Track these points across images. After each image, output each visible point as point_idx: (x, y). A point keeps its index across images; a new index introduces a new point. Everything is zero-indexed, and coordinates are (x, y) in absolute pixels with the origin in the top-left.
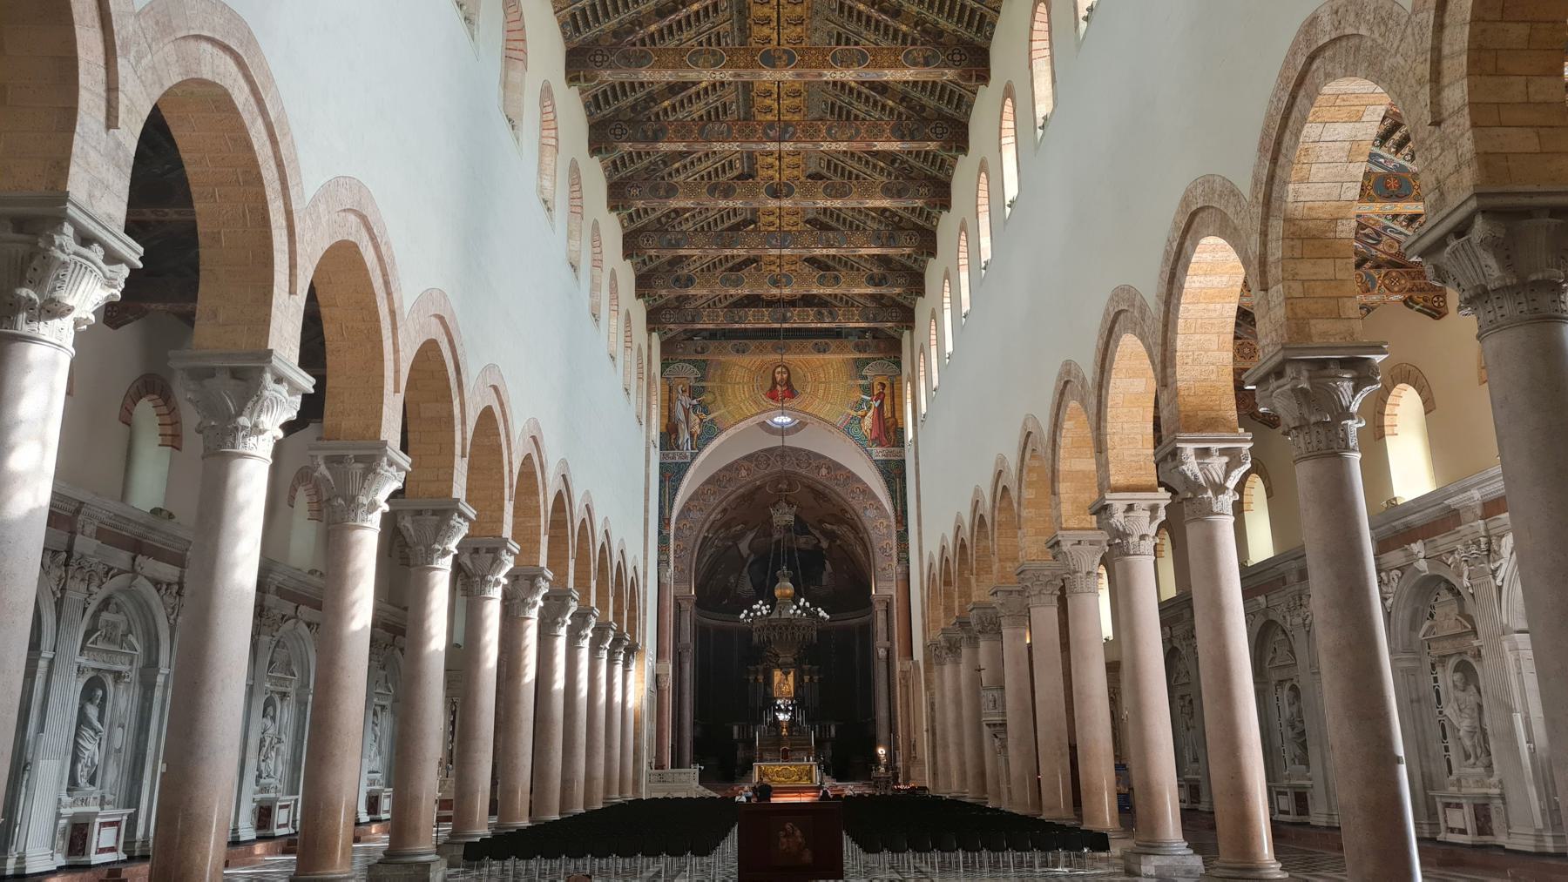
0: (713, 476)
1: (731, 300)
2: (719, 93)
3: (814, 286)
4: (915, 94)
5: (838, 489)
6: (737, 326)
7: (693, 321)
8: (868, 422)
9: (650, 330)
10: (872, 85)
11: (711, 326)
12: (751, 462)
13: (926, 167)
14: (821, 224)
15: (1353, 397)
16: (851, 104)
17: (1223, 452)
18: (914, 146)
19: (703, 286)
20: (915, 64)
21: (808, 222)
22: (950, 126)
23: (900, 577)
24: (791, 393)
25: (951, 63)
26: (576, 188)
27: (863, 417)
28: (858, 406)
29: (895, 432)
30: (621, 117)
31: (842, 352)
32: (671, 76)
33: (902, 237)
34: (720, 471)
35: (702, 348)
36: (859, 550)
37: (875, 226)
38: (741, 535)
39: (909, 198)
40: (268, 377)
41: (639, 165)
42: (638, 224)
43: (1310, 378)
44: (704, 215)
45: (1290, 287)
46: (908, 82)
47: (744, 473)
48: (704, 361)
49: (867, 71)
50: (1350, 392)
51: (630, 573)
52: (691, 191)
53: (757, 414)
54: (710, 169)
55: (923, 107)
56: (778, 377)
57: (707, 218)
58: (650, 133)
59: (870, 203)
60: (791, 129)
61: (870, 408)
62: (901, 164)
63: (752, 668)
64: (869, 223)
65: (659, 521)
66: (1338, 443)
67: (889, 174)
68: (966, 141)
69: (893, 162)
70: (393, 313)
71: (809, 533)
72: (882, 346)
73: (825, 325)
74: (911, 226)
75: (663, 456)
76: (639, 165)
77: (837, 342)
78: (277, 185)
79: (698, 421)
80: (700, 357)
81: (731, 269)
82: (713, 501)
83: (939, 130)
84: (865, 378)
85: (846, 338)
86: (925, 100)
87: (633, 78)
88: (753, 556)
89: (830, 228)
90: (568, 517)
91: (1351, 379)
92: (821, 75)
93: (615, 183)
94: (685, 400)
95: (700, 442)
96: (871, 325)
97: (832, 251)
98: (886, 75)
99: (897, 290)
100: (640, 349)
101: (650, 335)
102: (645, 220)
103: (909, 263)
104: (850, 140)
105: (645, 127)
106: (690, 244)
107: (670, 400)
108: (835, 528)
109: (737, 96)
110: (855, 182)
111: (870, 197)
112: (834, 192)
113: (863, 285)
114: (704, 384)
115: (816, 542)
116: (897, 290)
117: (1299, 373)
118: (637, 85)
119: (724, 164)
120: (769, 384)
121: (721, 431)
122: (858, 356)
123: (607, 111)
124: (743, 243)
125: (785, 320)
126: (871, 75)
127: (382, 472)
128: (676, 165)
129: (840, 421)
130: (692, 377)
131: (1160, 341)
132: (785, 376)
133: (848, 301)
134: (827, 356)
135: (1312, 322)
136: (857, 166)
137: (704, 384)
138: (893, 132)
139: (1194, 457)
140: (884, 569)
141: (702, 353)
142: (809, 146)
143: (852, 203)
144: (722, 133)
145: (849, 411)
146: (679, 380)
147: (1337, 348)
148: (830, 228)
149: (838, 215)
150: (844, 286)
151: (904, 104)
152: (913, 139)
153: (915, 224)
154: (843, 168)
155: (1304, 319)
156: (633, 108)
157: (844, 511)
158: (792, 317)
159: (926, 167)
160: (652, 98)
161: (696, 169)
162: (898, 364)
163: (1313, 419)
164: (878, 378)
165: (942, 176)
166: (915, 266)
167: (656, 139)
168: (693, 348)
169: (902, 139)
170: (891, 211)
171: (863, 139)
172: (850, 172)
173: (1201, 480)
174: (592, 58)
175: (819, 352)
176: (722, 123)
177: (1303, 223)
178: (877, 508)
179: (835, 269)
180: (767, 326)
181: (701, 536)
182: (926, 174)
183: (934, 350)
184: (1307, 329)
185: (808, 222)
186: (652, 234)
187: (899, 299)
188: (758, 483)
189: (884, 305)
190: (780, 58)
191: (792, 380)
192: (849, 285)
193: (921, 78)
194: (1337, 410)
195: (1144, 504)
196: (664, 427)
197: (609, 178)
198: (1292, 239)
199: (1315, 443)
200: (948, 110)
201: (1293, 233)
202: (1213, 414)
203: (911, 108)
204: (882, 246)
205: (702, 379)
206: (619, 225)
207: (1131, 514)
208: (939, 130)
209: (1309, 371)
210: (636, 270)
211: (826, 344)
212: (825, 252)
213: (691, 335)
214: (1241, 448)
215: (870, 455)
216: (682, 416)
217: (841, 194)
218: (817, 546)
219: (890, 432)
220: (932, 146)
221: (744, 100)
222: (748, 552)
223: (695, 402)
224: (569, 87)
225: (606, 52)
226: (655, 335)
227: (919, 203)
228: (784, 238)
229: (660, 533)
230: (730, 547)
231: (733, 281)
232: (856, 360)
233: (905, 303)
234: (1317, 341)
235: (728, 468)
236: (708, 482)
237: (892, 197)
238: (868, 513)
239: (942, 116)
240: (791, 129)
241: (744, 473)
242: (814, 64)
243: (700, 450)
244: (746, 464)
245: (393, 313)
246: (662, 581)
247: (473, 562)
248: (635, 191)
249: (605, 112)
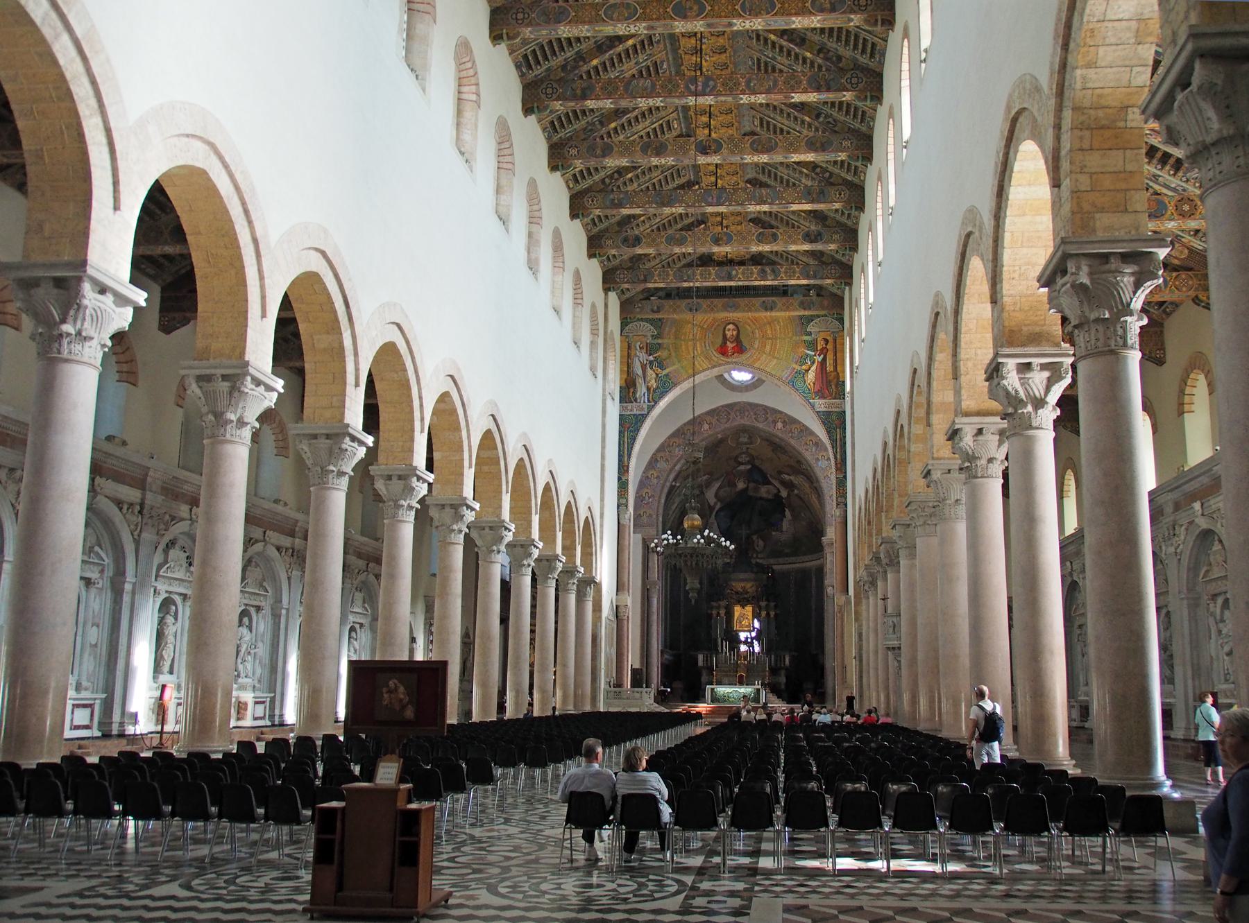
0: (678, 430)
1: (684, 262)
2: (648, 52)
3: (753, 243)
4: (832, 44)
5: (793, 442)
6: (686, 285)
7: (645, 281)
8: (811, 376)
9: (606, 290)
10: (783, 33)
11: (662, 285)
12: (713, 417)
13: (849, 119)
14: (760, 182)
15: (1135, 293)
16: (774, 58)
17: (1044, 367)
18: (830, 96)
19: (649, 246)
20: (822, 10)
21: (749, 181)
22: (865, 76)
23: (839, 520)
24: (740, 349)
25: (856, 8)
26: (506, 145)
27: (807, 371)
28: (802, 360)
29: (836, 387)
30: (552, 77)
31: (787, 309)
32: (588, 30)
33: (832, 191)
34: (685, 424)
35: (658, 308)
36: (814, 498)
37: (809, 183)
38: (708, 484)
39: (833, 151)
40: (87, 287)
41: (578, 126)
42: (584, 185)
43: (1091, 274)
44: (648, 177)
45: (1077, 180)
46: (815, 29)
47: (706, 426)
48: (660, 320)
49: (776, 18)
50: (1131, 289)
51: (583, 514)
52: (626, 149)
53: (708, 369)
54: (648, 130)
55: (840, 58)
56: (729, 334)
57: (651, 179)
58: (579, 92)
59: (796, 158)
60: (711, 83)
61: (813, 363)
62: (825, 117)
63: (714, 604)
64: (803, 180)
65: (619, 469)
66: (1116, 341)
67: (817, 130)
68: (881, 90)
69: (818, 116)
70: (255, 241)
71: (769, 483)
72: (826, 303)
73: (768, 283)
74: (841, 182)
75: (622, 408)
76: (578, 126)
77: (784, 299)
78: (93, 102)
79: (654, 375)
80: (656, 316)
81: (681, 230)
82: (678, 452)
83: (854, 80)
84: (810, 334)
85: (792, 295)
86: (842, 51)
87: (553, 36)
89: (766, 185)
90: (501, 454)
91: (1133, 274)
92: (730, 25)
93: (556, 144)
94: (641, 356)
95: (656, 395)
96: (812, 282)
97: (766, 208)
98: (794, 22)
99: (832, 247)
100: (593, 306)
101: (606, 294)
102: (589, 182)
103: (844, 220)
104: (768, 92)
105: (574, 86)
106: (632, 204)
107: (629, 356)
108: (792, 478)
109: (667, 54)
110: (781, 137)
111: (795, 151)
112: (760, 148)
113: (799, 242)
114: (660, 341)
115: (776, 491)
116: (832, 247)
117: (1078, 268)
118: (564, 44)
119: (662, 125)
120: (719, 341)
121: (675, 385)
122: (802, 313)
123: (539, 71)
124: (681, 202)
125: (730, 278)
126: (780, 23)
127: (246, 390)
128: (613, 125)
129: (785, 374)
130: (649, 334)
131: (991, 258)
132: (735, 333)
133: (791, 259)
134: (773, 314)
135: (1098, 216)
136: (786, 122)
137: (660, 341)
138: (809, 82)
139: (1015, 372)
141: (658, 311)
142: (730, 99)
143: (778, 158)
144: (646, 89)
145: (795, 366)
146: (638, 338)
147: (1119, 241)
148: (766, 185)
149: (776, 175)
150: (781, 243)
151: (821, 55)
152: (828, 90)
153: (844, 179)
154: (775, 126)
155: (1089, 213)
156: (564, 67)
157: (799, 462)
158: (736, 275)
159: (849, 119)
160: (581, 58)
161: (634, 130)
162: (841, 320)
163: (1092, 316)
164: (822, 334)
165: (864, 129)
166: (849, 223)
167: (584, 97)
168: (650, 307)
169: (818, 89)
170: (821, 167)
171: (780, 92)
172: (782, 130)
173: (1022, 395)
174: (514, 16)
175: (766, 309)
176: (646, 79)
177: (1092, 112)
179: (772, 227)
180: (714, 284)
181: (668, 484)
182: (849, 128)
183: (863, 301)
184: (1091, 224)
185: (749, 181)
186: (596, 194)
187: (838, 257)
188: (720, 436)
189: (824, 263)
190: (691, 8)
191: (741, 336)
192: (786, 243)
193: (827, 25)
194: (1117, 307)
195: (993, 428)
196: (623, 382)
197: (549, 139)
198: (1081, 129)
199: (1093, 342)
200: (864, 60)
201: (1082, 123)
202: (1037, 329)
203: (826, 59)
204: (812, 202)
205: (659, 336)
206: (566, 190)
207: (980, 438)
208: (854, 80)
209: (1090, 266)
210: (587, 231)
211: (773, 301)
212: (758, 208)
213: (648, 294)
214: (1061, 363)
215: (813, 406)
216: (640, 372)
217: (768, 150)
218: (778, 496)
219: (832, 385)
220: (848, 96)
221: (674, 59)
223: (651, 358)
224: (494, 45)
225: (527, 10)
226: (613, 296)
227: (842, 156)
228: (722, 195)
229: (619, 479)
231: (677, 240)
232: (801, 317)
233: (843, 259)
234: (1100, 235)
236: (673, 435)
237: (816, 151)
239: (857, 66)
240: (711, 83)
241: (706, 426)
242: (723, 14)
243: (656, 403)
244: (708, 418)
245: (255, 241)
246: (621, 522)
247: (387, 489)
248: (574, 152)
249: (537, 72)
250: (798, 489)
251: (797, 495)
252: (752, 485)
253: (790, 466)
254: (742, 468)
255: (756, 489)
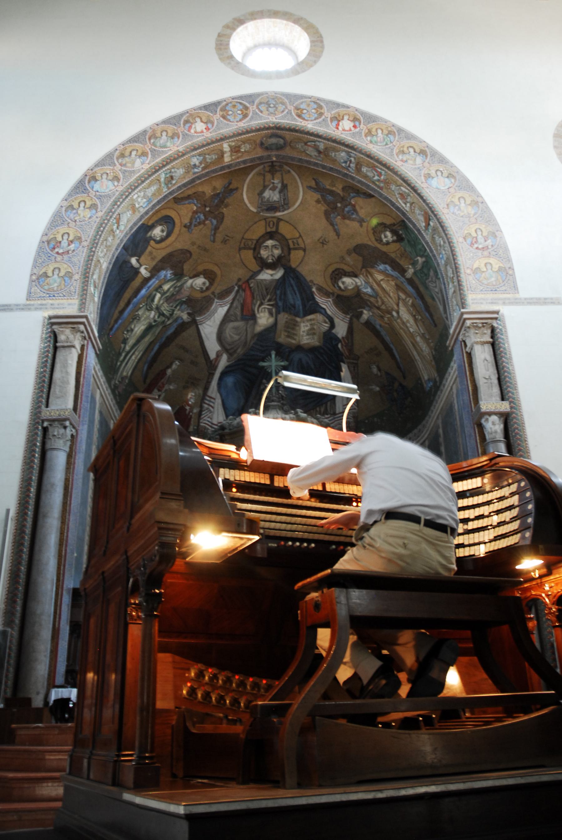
88: (225, 357)
140: (477, 270)
178: (450, 176)
222: (218, 348)
230: (183, 327)
235: (174, 120)
238: (434, 183)
244: (206, 114)
250: (371, 306)
251: (368, 324)
252: (283, 318)
253: (359, 249)
254: (266, 275)
255: (292, 327)
